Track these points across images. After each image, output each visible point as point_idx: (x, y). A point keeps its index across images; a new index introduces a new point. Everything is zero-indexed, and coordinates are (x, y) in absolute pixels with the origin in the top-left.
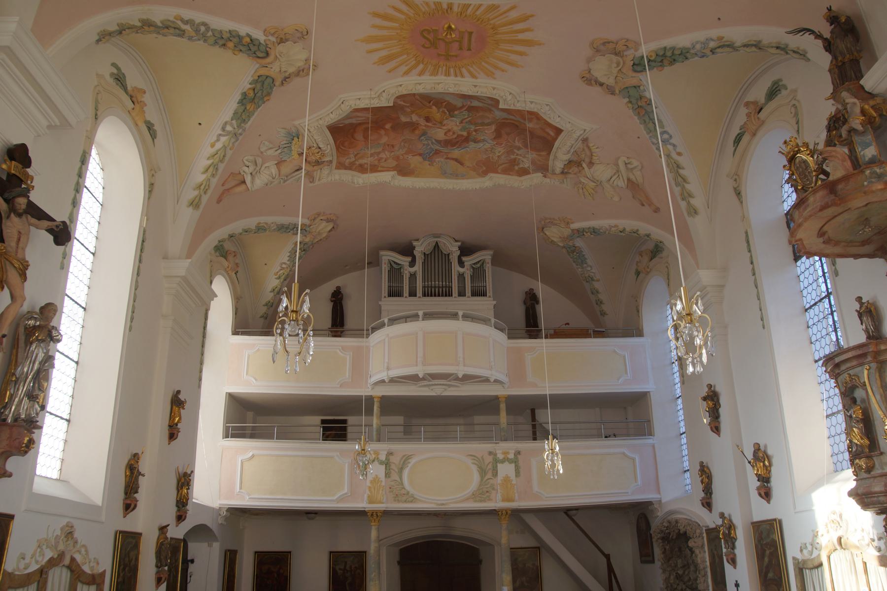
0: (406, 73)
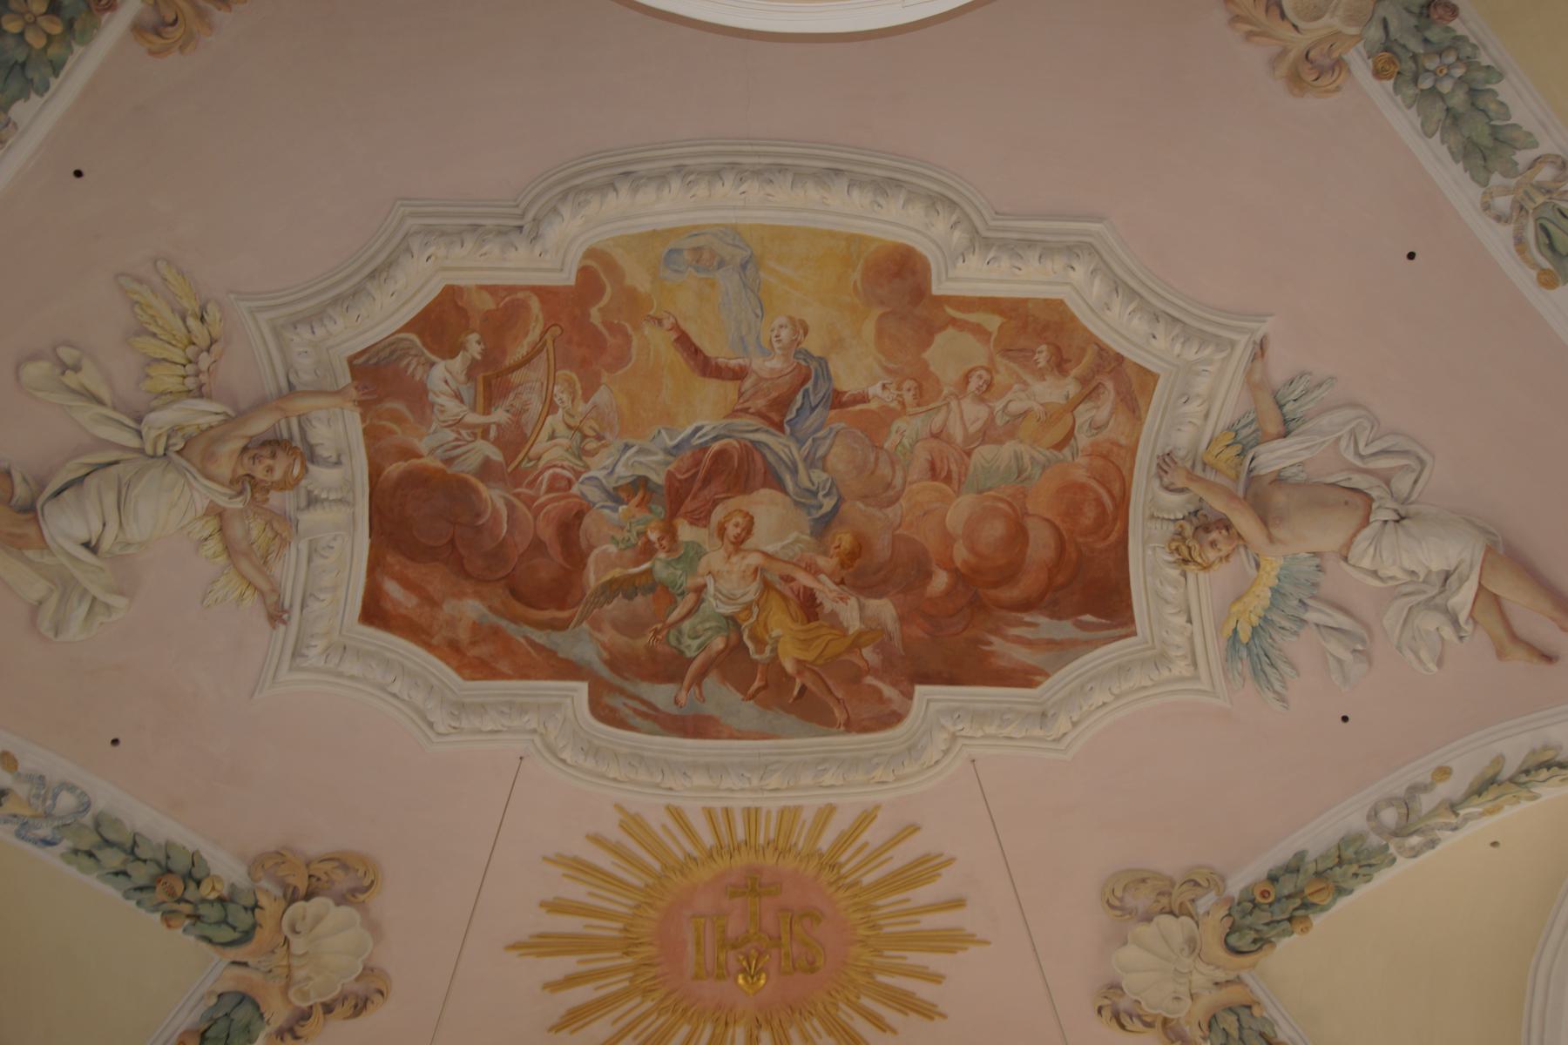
0: (866, 818)
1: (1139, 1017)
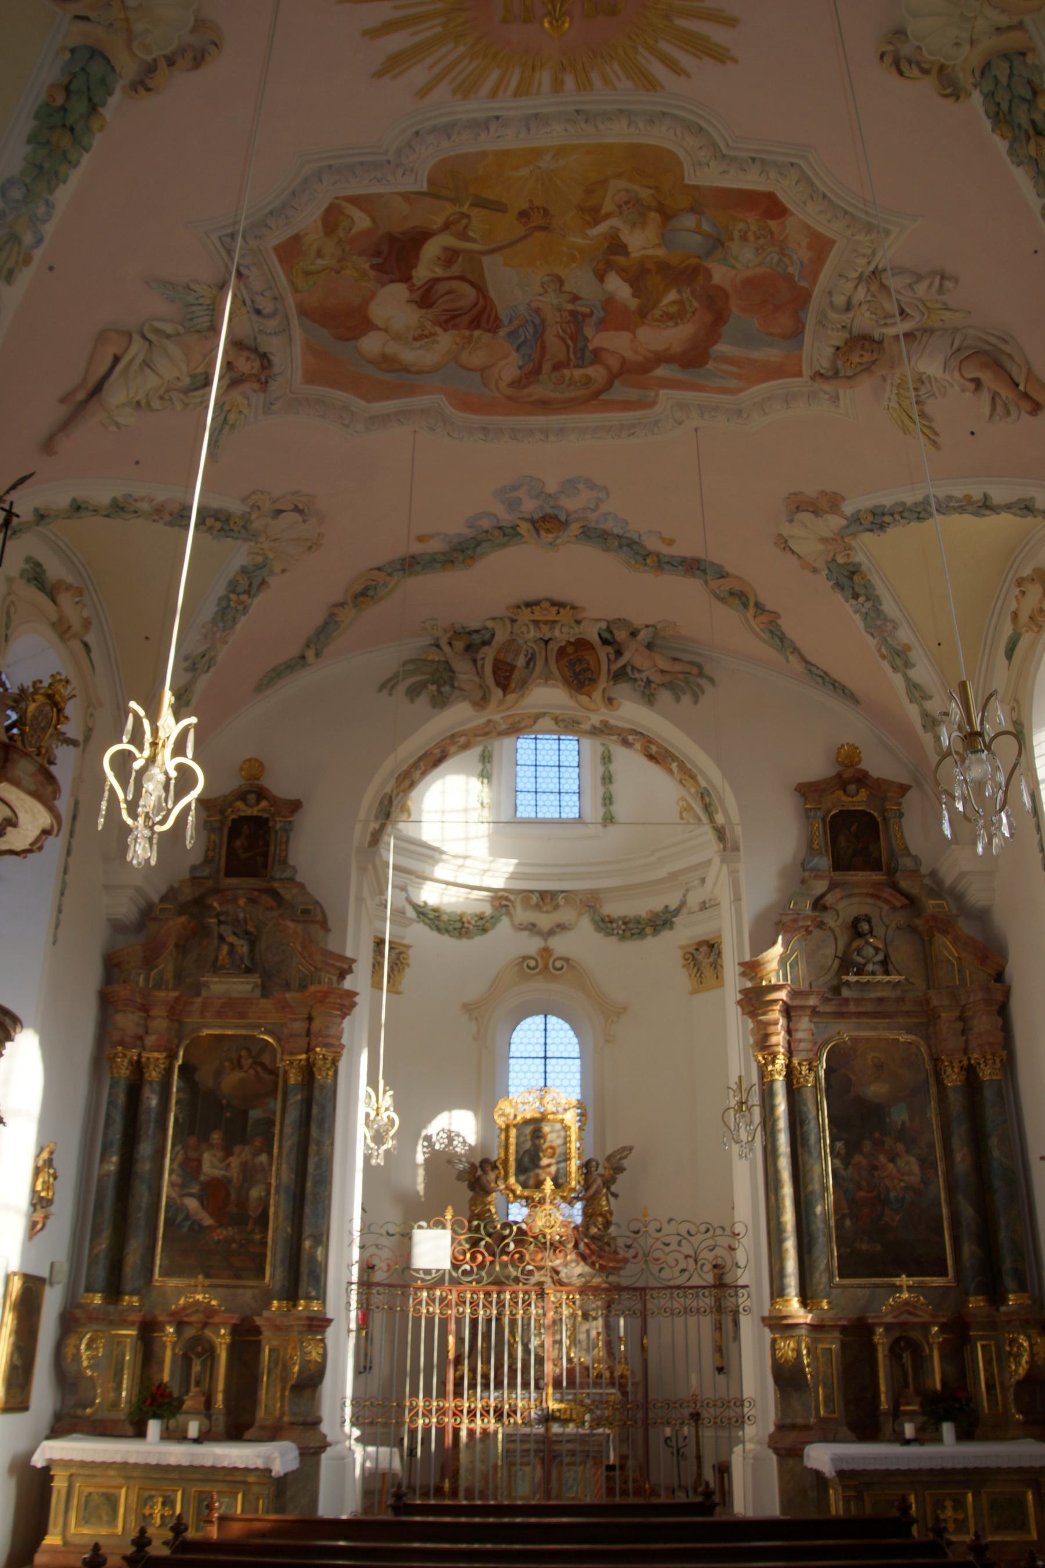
1: (918, 64)
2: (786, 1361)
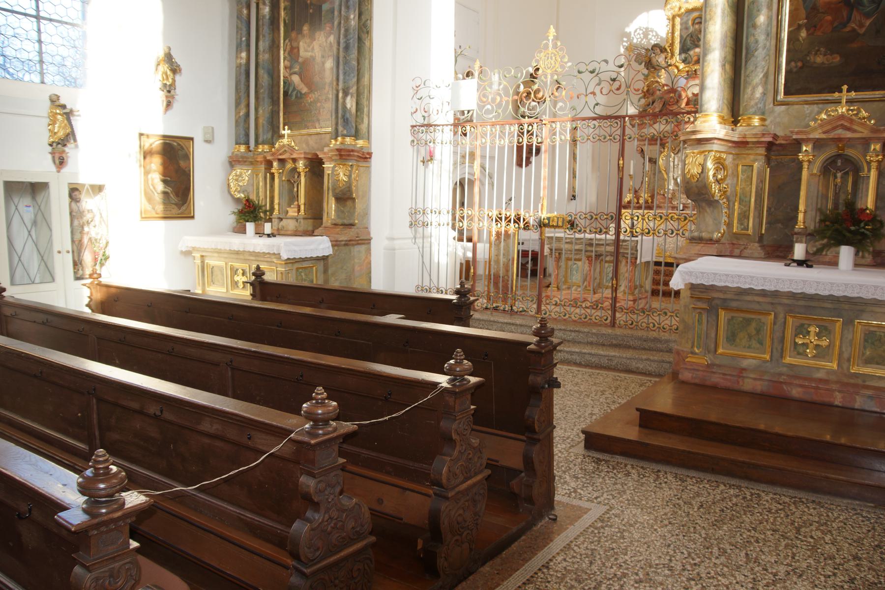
2: (692, 176)
